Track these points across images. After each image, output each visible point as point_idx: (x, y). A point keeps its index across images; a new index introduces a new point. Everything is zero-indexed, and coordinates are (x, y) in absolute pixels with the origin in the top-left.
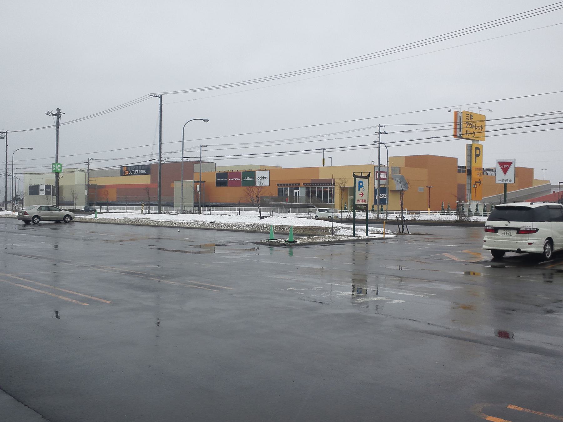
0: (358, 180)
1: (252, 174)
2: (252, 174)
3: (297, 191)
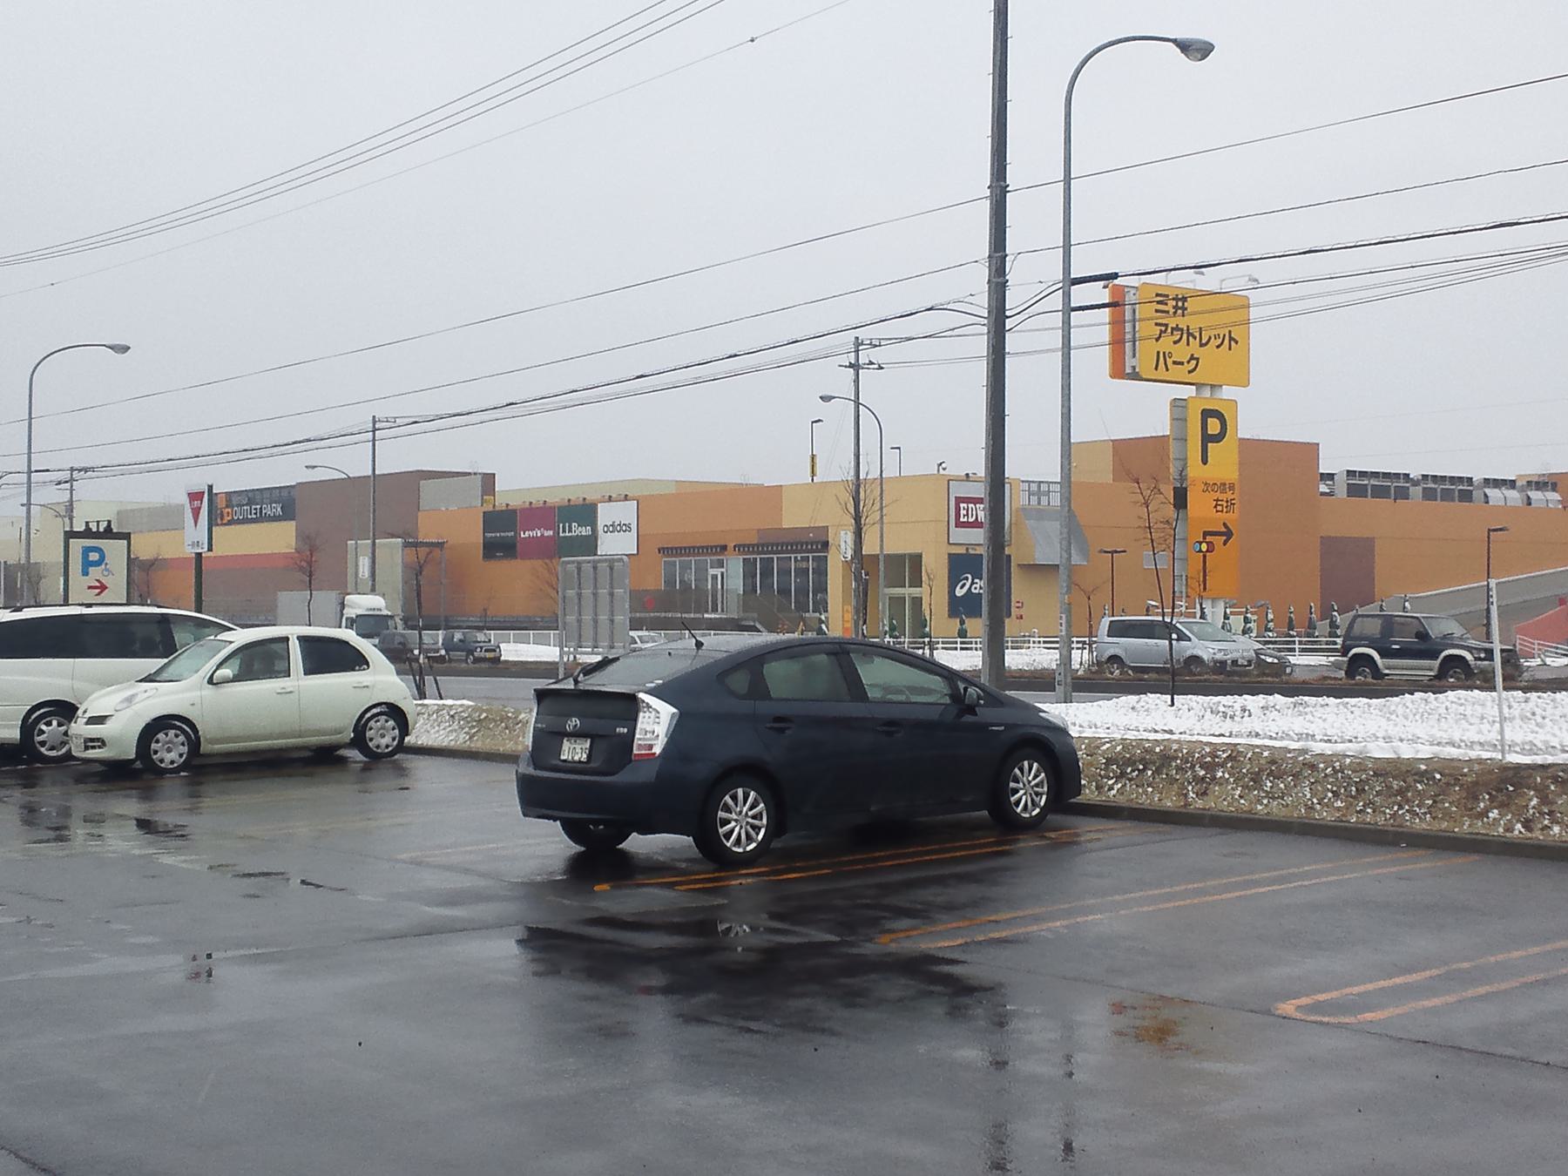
0: (77, 545)
1: (585, 512)
2: (585, 512)
3: (718, 571)
